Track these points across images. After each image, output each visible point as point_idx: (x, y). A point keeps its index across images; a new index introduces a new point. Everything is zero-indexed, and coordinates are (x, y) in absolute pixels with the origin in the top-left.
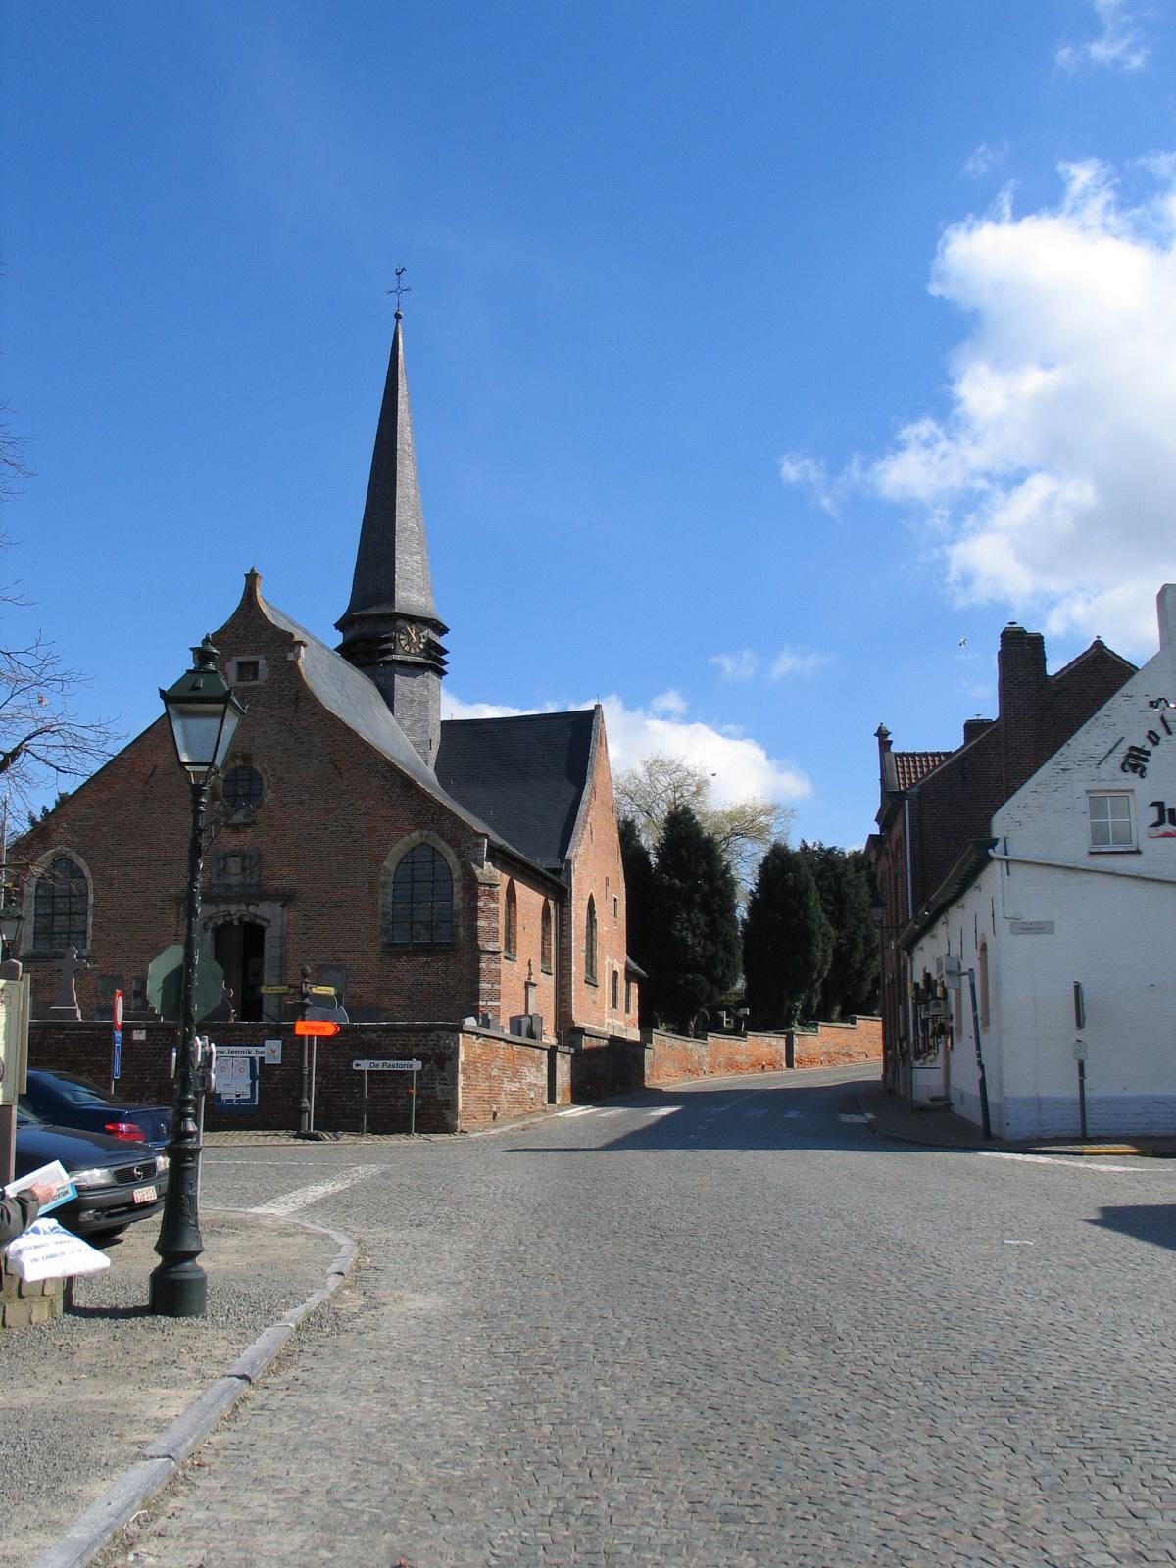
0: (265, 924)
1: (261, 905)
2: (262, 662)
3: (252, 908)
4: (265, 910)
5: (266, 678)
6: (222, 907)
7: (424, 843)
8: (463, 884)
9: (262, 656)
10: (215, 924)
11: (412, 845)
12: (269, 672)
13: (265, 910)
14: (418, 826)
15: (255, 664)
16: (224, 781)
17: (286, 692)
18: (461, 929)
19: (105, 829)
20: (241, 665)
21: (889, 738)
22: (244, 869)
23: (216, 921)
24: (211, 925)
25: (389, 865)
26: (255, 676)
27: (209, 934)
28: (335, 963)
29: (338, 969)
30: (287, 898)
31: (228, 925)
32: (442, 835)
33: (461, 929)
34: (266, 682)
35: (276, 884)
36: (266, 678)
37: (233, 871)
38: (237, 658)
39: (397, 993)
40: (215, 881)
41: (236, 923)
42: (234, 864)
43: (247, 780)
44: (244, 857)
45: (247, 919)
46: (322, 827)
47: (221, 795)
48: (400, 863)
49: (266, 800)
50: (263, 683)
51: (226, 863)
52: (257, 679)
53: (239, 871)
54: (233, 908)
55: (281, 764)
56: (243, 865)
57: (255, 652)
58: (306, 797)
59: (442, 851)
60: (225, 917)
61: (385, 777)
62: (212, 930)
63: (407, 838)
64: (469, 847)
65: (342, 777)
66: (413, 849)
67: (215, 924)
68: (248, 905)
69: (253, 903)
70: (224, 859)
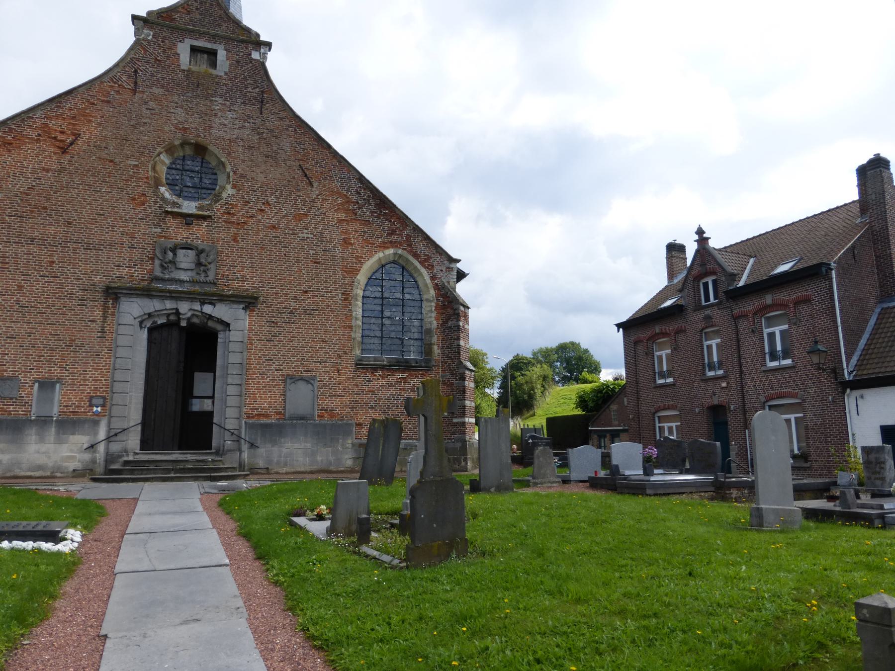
0: (219, 327)
1: (218, 306)
2: (222, 54)
3: (208, 309)
4: (220, 311)
5: (227, 70)
6: (169, 305)
7: (394, 262)
8: (437, 304)
9: (222, 46)
10: (154, 322)
11: (383, 262)
12: (231, 65)
13: (220, 311)
14: (393, 244)
15: (213, 54)
16: (169, 168)
17: (249, 90)
18: (436, 347)
20: (194, 50)
21: (705, 235)
22: (199, 264)
23: (156, 319)
24: (148, 324)
25: (362, 278)
26: (214, 64)
27: (144, 334)
28: (304, 374)
29: (308, 381)
30: (249, 302)
31: (172, 324)
32: (416, 256)
33: (436, 347)
34: (226, 74)
35: (236, 284)
36: (227, 70)
37: (183, 265)
39: (372, 408)
40: (161, 275)
41: (184, 324)
42: (186, 259)
43: (198, 172)
44: (200, 252)
45: (195, 320)
46: (291, 232)
47: (164, 181)
48: (370, 279)
50: (222, 74)
51: (175, 254)
52: (215, 68)
53: (192, 266)
54: (185, 308)
55: (244, 161)
56: (199, 260)
57: (214, 38)
58: (272, 199)
59: (413, 272)
60: (168, 315)
61: (358, 193)
62: (151, 330)
63: (381, 255)
64: (441, 270)
65: (311, 184)
66: (383, 266)
67: (154, 322)
68: (203, 303)
69: (210, 303)
70: (174, 250)
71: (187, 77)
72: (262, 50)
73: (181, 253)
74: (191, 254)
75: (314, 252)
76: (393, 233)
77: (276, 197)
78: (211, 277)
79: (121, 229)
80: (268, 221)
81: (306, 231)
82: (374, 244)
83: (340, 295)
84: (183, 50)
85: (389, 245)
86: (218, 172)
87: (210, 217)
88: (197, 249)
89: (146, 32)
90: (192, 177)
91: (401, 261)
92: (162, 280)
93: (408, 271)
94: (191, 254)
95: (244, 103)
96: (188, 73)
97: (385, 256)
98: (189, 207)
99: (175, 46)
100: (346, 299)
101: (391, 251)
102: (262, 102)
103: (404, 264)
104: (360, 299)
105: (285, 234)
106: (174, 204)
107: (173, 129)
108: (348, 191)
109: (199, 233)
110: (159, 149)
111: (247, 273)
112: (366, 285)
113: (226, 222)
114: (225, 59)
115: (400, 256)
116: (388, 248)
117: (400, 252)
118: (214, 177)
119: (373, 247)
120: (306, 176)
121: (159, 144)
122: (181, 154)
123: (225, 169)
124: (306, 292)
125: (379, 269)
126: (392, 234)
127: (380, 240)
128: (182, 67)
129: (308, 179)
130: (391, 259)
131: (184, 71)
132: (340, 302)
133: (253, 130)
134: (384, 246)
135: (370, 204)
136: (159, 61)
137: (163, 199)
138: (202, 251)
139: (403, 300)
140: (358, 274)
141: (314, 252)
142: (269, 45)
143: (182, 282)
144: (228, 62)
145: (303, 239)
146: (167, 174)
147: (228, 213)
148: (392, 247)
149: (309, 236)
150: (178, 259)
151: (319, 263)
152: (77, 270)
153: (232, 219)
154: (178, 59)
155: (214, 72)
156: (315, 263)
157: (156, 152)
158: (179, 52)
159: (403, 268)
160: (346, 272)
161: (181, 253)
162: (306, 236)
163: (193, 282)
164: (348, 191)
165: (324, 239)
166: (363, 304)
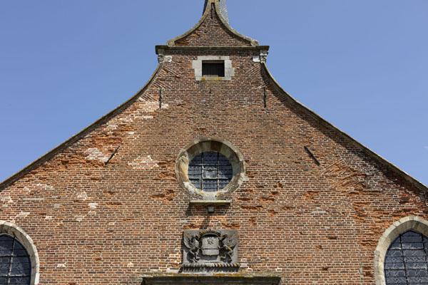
7: (410, 231)
19: (57, 206)
20: (205, 64)
22: (223, 251)
26: (222, 74)
34: (233, 78)
37: (208, 252)
38: (201, 58)
40: (186, 262)
42: (211, 246)
47: (187, 177)
49: (240, 183)
50: (230, 79)
51: (201, 243)
52: (224, 76)
53: (217, 252)
58: (283, 181)
65: (318, 163)
71: (202, 86)
72: (261, 54)
73: (205, 241)
74: (215, 241)
75: (329, 228)
76: (404, 201)
77: (286, 179)
78: (234, 262)
79: (154, 224)
80: (281, 202)
81: (318, 208)
82: (388, 214)
83: (361, 269)
84: (197, 64)
85: (403, 214)
86: (232, 163)
87: (229, 204)
88: (219, 235)
89: (167, 57)
90: (210, 171)
91: (419, 229)
92: (191, 268)
93: (425, 237)
94: (215, 241)
95: (251, 100)
96: (201, 83)
97: (402, 225)
98: (211, 196)
99: (190, 63)
100: (368, 274)
101: (407, 219)
102: (265, 96)
103: (423, 232)
104: (382, 272)
105: (300, 213)
106: (197, 196)
107: (192, 130)
108: (353, 165)
109: (218, 222)
110: (183, 150)
111: (266, 254)
112: (386, 257)
113: (243, 208)
114: (231, 67)
115: (418, 223)
116: (403, 217)
117: (416, 219)
118: (228, 168)
119: (385, 215)
120: (311, 156)
121: (181, 145)
122: (200, 152)
123: (238, 159)
124: (326, 269)
125: (397, 239)
126: (405, 202)
127: (394, 209)
128: (198, 79)
129: (313, 158)
130: (409, 228)
131: (198, 82)
132: (362, 276)
133: (260, 121)
134: (398, 214)
135: (377, 174)
136: (178, 78)
137: (187, 192)
138: (225, 237)
139: (405, 270)
140: (376, 246)
141: (329, 228)
142: (266, 48)
143: (208, 268)
144: (234, 69)
145: (317, 216)
146: (189, 170)
147: (244, 199)
148: (407, 215)
149: (322, 212)
150: (204, 247)
151: (335, 238)
152: (119, 265)
153: (249, 205)
154: (193, 74)
155: (223, 78)
156: (331, 238)
157: (181, 151)
158: (193, 68)
159: (422, 235)
160: (364, 245)
161: (205, 241)
162: (318, 212)
163: (218, 268)
164: (353, 165)
165: (337, 214)
166: (386, 277)
